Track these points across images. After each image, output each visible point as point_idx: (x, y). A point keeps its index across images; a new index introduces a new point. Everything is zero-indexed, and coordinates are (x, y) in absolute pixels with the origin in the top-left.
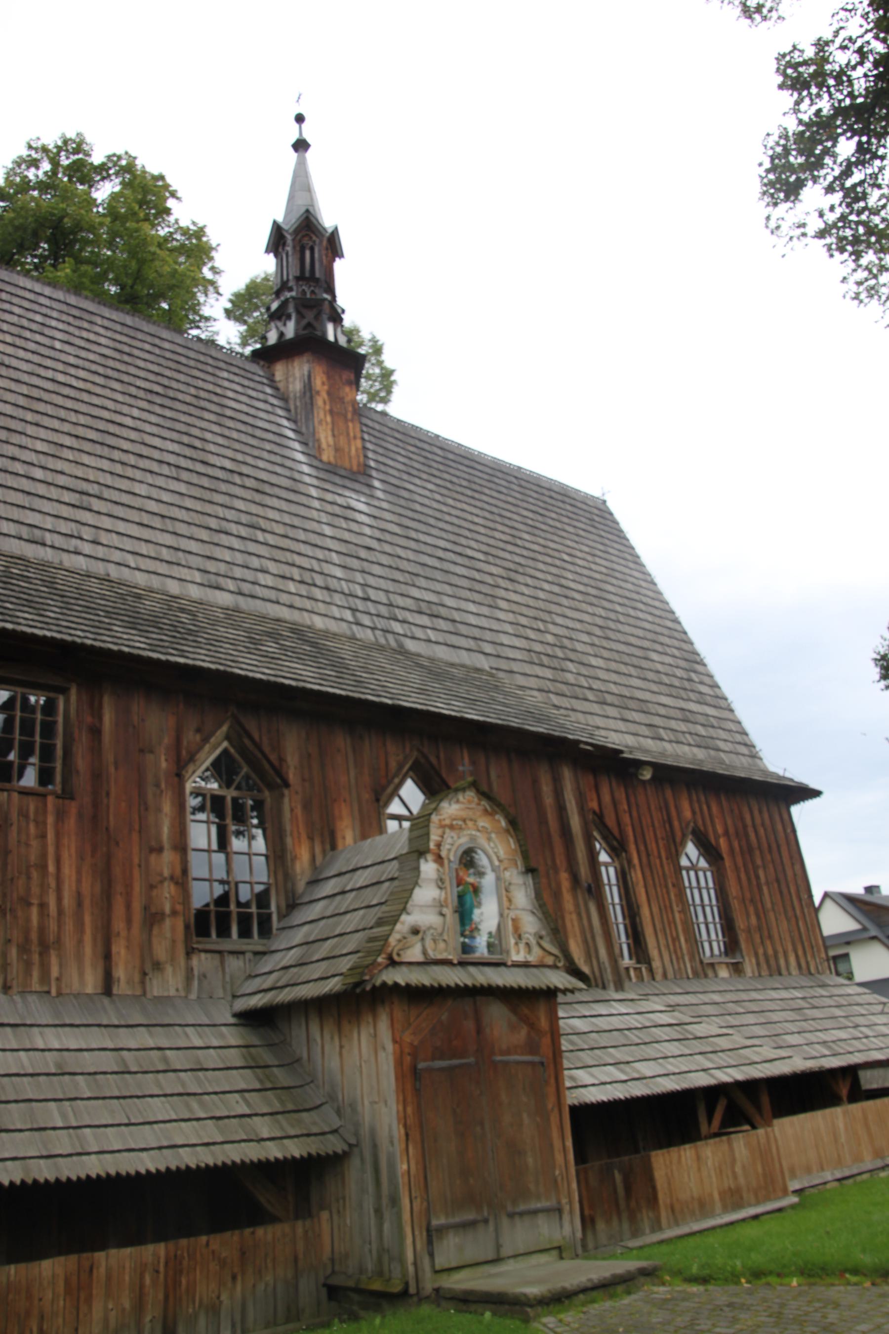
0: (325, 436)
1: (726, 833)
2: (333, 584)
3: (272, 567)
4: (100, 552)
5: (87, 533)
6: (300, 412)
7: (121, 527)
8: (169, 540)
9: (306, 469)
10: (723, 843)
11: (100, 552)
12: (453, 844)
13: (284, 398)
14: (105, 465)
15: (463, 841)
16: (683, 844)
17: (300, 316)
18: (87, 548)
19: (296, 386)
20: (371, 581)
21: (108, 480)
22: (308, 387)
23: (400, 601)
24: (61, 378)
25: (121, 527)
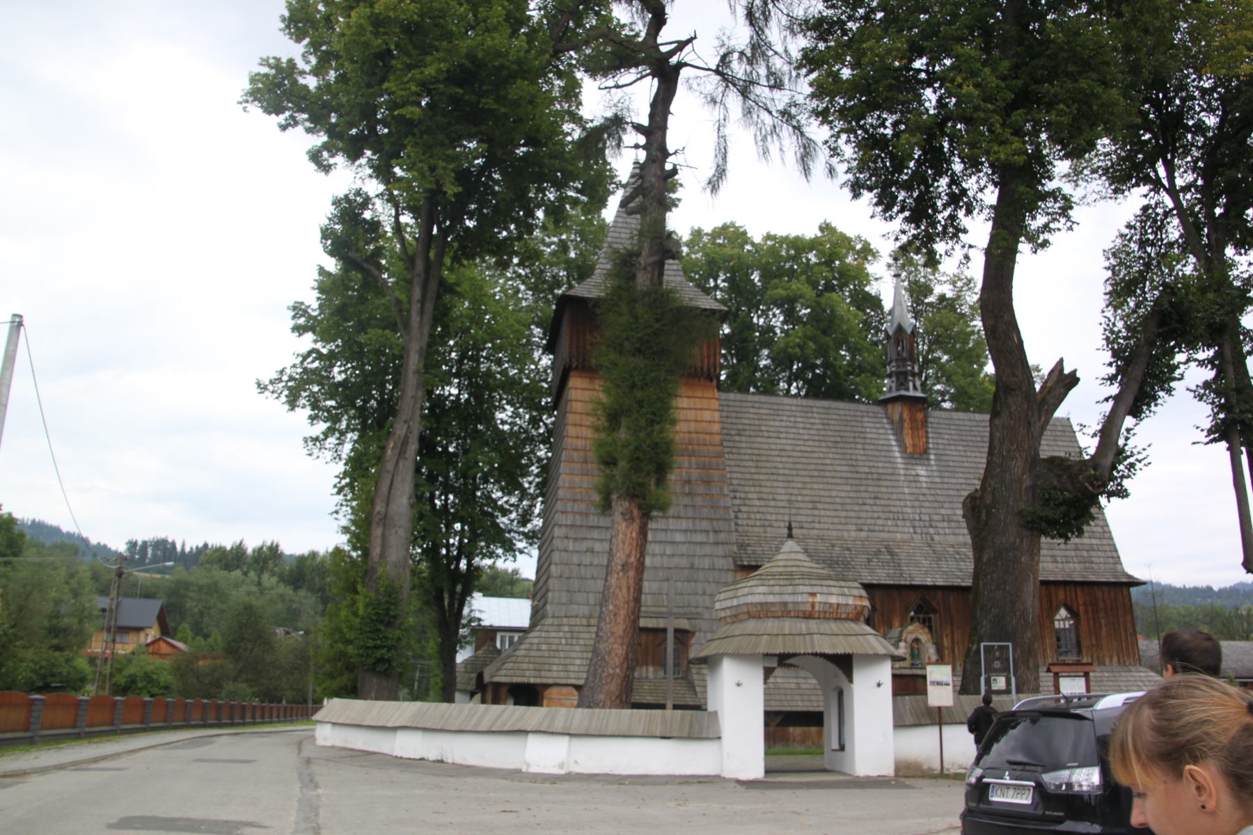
0: (908, 441)
1: (1085, 604)
2: (907, 516)
3: (882, 515)
4: (821, 526)
5: (817, 519)
6: (898, 432)
7: (828, 513)
8: (843, 514)
9: (900, 460)
10: (1081, 609)
11: (821, 526)
12: (910, 637)
13: (892, 422)
14: (821, 486)
15: (913, 636)
16: (1057, 610)
17: (898, 379)
18: (817, 526)
19: (896, 417)
20: (924, 510)
21: (822, 493)
22: (901, 420)
23: (935, 517)
24: (803, 448)
25: (828, 513)
